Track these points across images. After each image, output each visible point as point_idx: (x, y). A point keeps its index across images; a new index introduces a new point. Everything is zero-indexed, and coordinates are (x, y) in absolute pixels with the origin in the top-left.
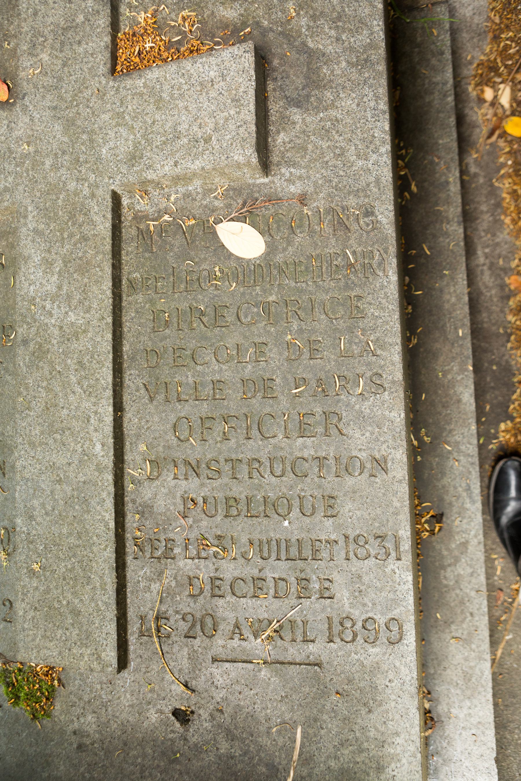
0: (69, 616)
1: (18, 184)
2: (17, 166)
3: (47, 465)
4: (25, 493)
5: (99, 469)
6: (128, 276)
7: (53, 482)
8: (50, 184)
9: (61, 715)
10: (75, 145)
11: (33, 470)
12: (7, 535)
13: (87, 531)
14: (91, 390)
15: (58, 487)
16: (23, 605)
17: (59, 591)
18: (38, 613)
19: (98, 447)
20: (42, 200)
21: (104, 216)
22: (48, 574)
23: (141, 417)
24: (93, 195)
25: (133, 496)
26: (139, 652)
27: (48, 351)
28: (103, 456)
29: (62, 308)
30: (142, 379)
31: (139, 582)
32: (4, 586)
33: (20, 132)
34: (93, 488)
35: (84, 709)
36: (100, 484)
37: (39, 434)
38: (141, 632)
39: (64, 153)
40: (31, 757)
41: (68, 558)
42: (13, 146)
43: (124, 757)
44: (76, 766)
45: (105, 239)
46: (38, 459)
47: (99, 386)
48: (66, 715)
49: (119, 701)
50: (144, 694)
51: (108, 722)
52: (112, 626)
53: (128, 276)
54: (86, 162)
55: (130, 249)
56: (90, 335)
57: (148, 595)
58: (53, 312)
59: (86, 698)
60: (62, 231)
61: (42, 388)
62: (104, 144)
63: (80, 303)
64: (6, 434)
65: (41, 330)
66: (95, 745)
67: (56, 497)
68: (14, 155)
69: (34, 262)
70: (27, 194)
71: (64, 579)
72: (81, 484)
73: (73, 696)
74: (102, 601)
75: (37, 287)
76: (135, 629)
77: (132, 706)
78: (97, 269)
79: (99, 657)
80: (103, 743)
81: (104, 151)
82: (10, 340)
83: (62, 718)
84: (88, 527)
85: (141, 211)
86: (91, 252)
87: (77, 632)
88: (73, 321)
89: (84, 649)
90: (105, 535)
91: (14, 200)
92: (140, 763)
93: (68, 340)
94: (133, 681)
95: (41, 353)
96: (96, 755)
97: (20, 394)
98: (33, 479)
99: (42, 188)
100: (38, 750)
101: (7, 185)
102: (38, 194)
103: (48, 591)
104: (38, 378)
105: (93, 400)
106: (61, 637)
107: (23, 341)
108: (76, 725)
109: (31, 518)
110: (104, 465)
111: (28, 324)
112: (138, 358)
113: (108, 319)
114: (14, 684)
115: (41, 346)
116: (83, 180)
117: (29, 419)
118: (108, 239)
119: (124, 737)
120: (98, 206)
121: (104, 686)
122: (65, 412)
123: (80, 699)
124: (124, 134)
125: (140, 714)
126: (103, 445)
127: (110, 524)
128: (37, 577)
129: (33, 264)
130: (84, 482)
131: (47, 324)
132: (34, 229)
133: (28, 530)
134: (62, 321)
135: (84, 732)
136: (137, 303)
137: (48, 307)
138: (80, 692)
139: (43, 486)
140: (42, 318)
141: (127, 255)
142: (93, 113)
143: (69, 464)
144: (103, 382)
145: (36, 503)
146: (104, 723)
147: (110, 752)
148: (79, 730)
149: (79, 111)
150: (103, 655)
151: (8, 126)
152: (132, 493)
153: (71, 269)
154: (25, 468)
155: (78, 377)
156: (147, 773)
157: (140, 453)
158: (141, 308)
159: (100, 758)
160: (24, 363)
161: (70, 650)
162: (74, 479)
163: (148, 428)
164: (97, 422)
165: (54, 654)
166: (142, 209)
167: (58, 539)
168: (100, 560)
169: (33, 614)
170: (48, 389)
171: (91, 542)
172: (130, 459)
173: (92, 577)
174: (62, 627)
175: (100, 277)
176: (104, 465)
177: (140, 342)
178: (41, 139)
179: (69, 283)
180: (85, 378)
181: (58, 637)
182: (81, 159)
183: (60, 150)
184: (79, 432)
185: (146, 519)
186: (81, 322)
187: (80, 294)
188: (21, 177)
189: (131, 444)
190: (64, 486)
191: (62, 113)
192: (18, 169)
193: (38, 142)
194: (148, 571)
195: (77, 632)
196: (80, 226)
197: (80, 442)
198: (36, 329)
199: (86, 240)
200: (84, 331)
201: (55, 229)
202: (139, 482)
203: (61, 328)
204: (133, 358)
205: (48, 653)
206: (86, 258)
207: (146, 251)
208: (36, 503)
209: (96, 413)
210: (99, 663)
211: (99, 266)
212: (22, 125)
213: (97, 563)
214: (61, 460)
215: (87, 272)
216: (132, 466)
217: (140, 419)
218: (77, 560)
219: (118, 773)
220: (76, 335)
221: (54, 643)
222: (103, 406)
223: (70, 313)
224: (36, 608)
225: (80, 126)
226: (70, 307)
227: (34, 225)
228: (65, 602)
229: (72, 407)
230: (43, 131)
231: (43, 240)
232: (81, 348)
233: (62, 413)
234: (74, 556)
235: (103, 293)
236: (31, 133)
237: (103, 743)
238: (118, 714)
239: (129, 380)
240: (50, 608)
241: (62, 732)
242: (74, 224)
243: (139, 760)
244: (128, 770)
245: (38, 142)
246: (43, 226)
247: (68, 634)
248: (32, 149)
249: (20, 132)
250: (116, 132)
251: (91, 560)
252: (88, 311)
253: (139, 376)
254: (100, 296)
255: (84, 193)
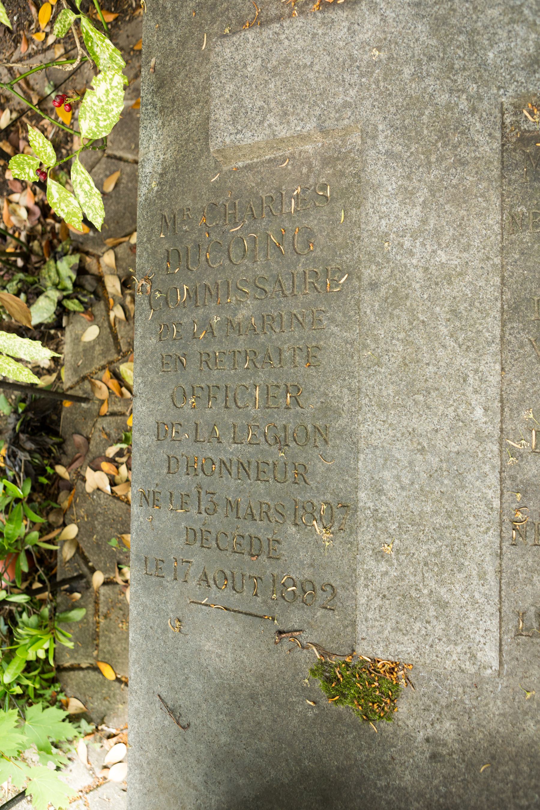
0: (432, 608)
1: (363, 98)
2: (362, 76)
3: (404, 430)
4: (372, 463)
5: (479, 437)
6: (511, 210)
7: (413, 451)
8: (411, 97)
9: (408, 718)
10: (448, 49)
11: (383, 437)
12: (330, 512)
13: (460, 511)
14: (469, 344)
15: (419, 457)
16: (366, 592)
17: (417, 578)
18: (387, 602)
19: (479, 412)
20: (398, 116)
21: (490, 135)
22: (402, 557)
23: (525, 379)
24: (474, 110)
25: (512, 472)
26: (517, 654)
27: (407, 296)
28: (486, 423)
29: (428, 246)
30: (528, 333)
31: (517, 572)
32: (324, 569)
33: (366, 36)
34: (470, 460)
35: (440, 714)
36: (480, 455)
37: (392, 394)
38: (517, 630)
39: (431, 58)
40: (360, 762)
41: (432, 541)
42: (356, 52)
43: (492, 772)
44: (428, 777)
45: (491, 162)
46: (391, 425)
47: (482, 340)
48: (416, 719)
49: (486, 708)
50: (519, 702)
51: (472, 731)
52: (494, 622)
53: (511, 210)
54: (464, 69)
55: (513, 177)
56: (467, 278)
57: (529, 588)
58: (414, 250)
59: (444, 702)
60: (427, 153)
61: (398, 340)
62: (492, 46)
63: (454, 240)
64: (331, 395)
65: (396, 272)
66: (454, 756)
67: (417, 469)
68: (357, 64)
69: (387, 191)
70: (375, 110)
71: (426, 564)
72: (452, 455)
73: (426, 699)
74: (480, 592)
75: (392, 221)
76: (510, 627)
77: (503, 715)
78: (480, 199)
79: (473, 657)
80: (464, 755)
81: (491, 55)
82: (337, 285)
83: (410, 722)
84: (461, 505)
85: (529, 131)
86: (471, 179)
87: (443, 626)
88: (444, 261)
89: (452, 646)
90: (487, 516)
91: (358, 117)
92: (512, 781)
93: (437, 284)
94: (507, 687)
95: (396, 299)
96: (455, 767)
97: (365, 346)
98: (383, 447)
99: (398, 102)
100: (371, 755)
101: (348, 99)
102: (393, 110)
103: (401, 578)
104: (393, 329)
105: (472, 355)
106: (419, 631)
107: (370, 284)
108: (430, 732)
109: (380, 492)
110: (486, 433)
111: (378, 264)
112: (523, 308)
113: (495, 259)
114: (339, 679)
115: (396, 290)
116: (459, 91)
117: (379, 377)
118: (495, 163)
119: (493, 750)
120: (480, 122)
121: (468, 690)
122: (432, 369)
123: (436, 703)
124: (521, 34)
125: (513, 725)
126: (486, 410)
127: (494, 504)
128: (387, 561)
129: (385, 194)
130: (458, 453)
131: (405, 265)
132: (387, 152)
133: (375, 505)
134: (428, 261)
135: (440, 740)
136: (523, 243)
137: (407, 244)
138: (436, 695)
139: (397, 455)
140: (399, 258)
141: (509, 184)
142: (475, 8)
143: (437, 431)
144: (487, 334)
145: (387, 475)
146: (466, 732)
147: (472, 765)
148: (433, 738)
149: (454, 7)
150: (479, 655)
151: (349, 29)
152: (510, 469)
153: (441, 199)
154: (372, 433)
155: (451, 328)
156: (521, 793)
157: (523, 422)
158: (528, 248)
159: (460, 771)
160: (372, 311)
161: (431, 646)
162: (443, 449)
163: (535, 392)
164: (477, 383)
165: (409, 649)
166: (531, 129)
167: (417, 518)
168: (478, 545)
169: (381, 603)
170: (406, 342)
171: (466, 522)
172: (509, 428)
173: (466, 563)
174: (422, 620)
175: (484, 208)
176: (486, 433)
177: (525, 290)
178: (396, 43)
179: (439, 216)
180: (461, 329)
181: (416, 631)
182: (457, 66)
183: (424, 55)
184: (451, 393)
185: (530, 499)
186: (456, 263)
187: (455, 229)
188: (368, 90)
189: (511, 410)
190: (429, 456)
191: (429, 10)
192: (363, 80)
193: (393, 46)
194: (530, 560)
195: (443, 626)
196: (455, 147)
197: (452, 405)
198: (389, 270)
199: (463, 164)
200: (460, 274)
201: (417, 152)
202: (521, 455)
203: (427, 269)
204: (516, 308)
205: (400, 648)
206: (463, 185)
207: (535, 180)
208: (387, 475)
209: (476, 371)
210: (474, 664)
211: (482, 196)
212: (369, 26)
213: (474, 548)
214: (425, 426)
215: (465, 202)
216: (511, 437)
217: (525, 381)
218: (445, 543)
219: (483, 790)
220: (447, 277)
221: (409, 637)
222: (487, 363)
223: (439, 252)
224: (384, 596)
225: (456, 25)
226: (439, 245)
227: (387, 146)
228: (426, 592)
229: (441, 363)
230: (400, 33)
231: (400, 164)
232: (455, 294)
233: (427, 370)
234: (441, 538)
235: (489, 227)
236: (382, 36)
237: (464, 755)
238: (485, 723)
239: (510, 334)
240: (404, 596)
241: (409, 738)
242: (445, 145)
243: (511, 777)
244: (497, 787)
245: (393, 46)
246: (400, 147)
247: (429, 628)
248: (383, 55)
249: (366, 36)
250: (510, 31)
251: (465, 545)
252: (466, 249)
253: (523, 330)
254: (484, 232)
255: (461, 107)
